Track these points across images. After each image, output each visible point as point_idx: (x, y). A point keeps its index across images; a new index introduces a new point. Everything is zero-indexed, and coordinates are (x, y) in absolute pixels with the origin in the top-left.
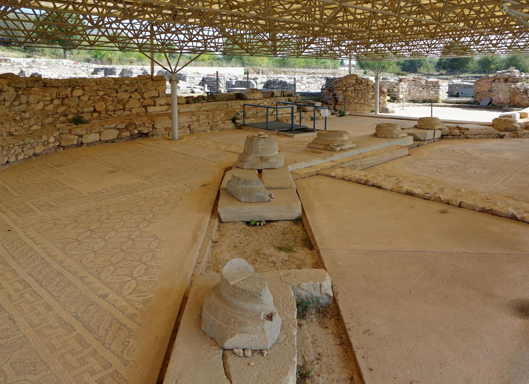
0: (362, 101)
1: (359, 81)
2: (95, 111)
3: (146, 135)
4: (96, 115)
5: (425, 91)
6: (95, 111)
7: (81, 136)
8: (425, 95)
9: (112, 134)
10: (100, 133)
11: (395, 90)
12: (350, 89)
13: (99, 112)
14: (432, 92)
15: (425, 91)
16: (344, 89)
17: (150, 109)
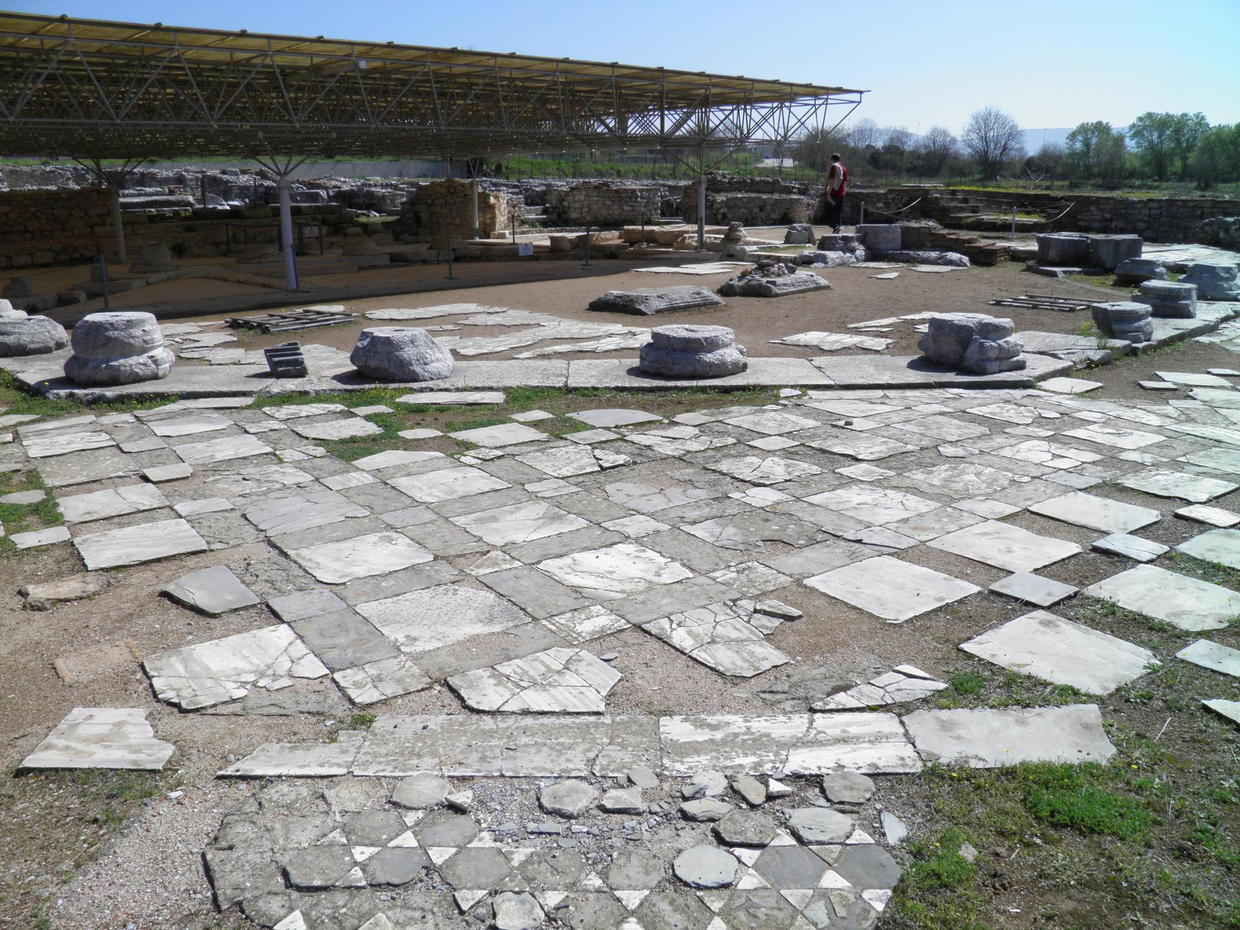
0: (458, 221)
1: (451, 188)
2: (26, 231)
3: (91, 259)
4: (28, 235)
5: (616, 207)
6: (26, 231)
7: (10, 258)
8: (617, 212)
9: (48, 257)
10: (31, 255)
11: (565, 204)
12: (437, 202)
13: (32, 232)
14: (626, 208)
15: (616, 207)
16: (429, 201)
17: (98, 230)
